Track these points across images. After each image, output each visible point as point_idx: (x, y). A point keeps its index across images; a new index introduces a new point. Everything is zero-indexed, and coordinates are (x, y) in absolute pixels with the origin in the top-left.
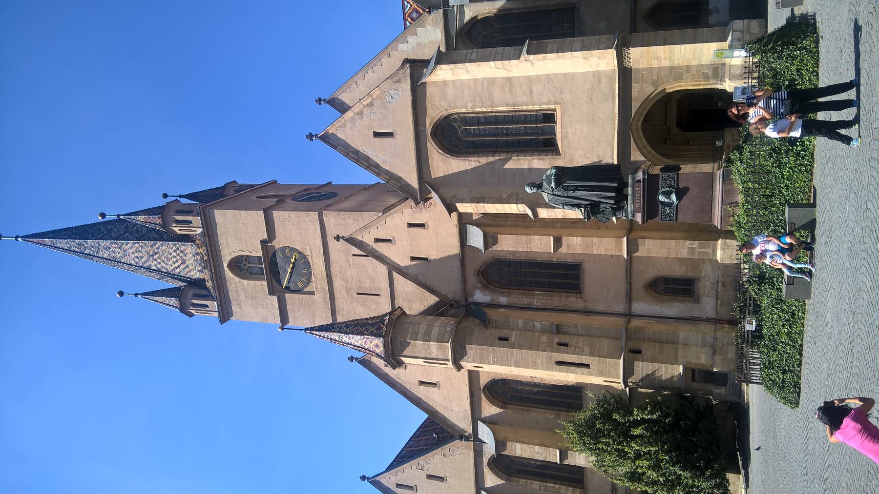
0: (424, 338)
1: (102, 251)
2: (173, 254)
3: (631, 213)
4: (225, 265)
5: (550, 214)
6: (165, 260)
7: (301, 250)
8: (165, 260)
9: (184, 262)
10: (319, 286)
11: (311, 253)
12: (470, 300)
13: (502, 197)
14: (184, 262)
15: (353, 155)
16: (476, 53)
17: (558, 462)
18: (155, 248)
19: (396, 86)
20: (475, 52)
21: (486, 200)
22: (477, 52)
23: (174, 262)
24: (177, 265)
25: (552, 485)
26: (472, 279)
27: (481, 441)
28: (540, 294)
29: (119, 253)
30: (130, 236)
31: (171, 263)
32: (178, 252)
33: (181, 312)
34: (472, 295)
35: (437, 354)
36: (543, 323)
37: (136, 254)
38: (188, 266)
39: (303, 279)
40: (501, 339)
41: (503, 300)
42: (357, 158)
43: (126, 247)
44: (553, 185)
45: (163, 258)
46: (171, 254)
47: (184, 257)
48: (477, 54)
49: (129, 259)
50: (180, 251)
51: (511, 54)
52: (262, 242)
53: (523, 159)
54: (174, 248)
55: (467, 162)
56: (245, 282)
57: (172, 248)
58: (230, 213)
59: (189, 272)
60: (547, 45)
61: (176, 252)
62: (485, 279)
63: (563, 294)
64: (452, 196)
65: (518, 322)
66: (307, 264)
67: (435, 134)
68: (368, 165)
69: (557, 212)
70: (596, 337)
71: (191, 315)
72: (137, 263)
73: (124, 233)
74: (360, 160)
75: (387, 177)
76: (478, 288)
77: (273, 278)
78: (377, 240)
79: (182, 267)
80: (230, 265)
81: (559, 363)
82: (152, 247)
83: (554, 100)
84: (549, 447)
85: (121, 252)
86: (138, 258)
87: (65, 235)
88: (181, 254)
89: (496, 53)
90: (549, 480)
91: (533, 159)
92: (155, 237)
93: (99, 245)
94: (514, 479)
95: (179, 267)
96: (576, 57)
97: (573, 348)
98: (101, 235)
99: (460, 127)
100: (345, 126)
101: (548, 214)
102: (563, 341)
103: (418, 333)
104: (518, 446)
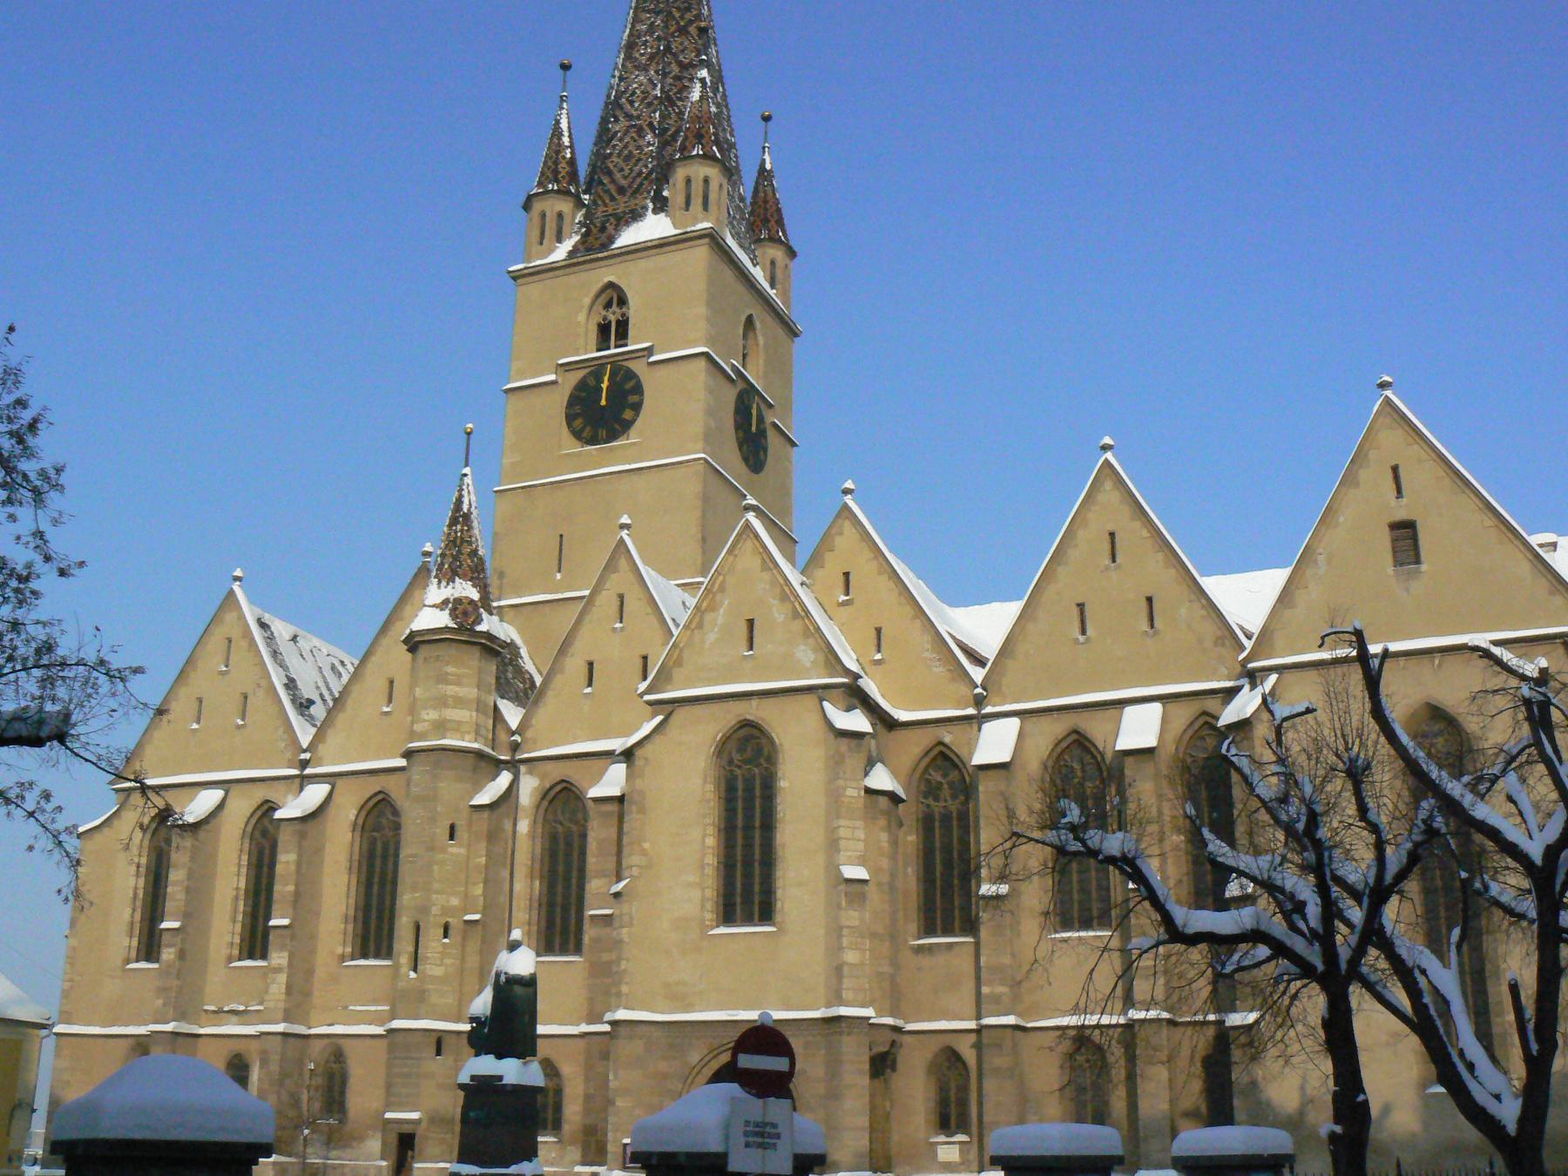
0: (451, 696)
1: (649, 18)
4: (612, 278)
7: (638, 424)
9: (621, 190)
12: (523, 768)
13: (645, 841)
14: (621, 190)
15: (718, 582)
16: (856, 795)
17: (272, 923)
19: (821, 658)
22: (859, 795)
23: (622, 170)
24: (618, 176)
25: (241, 908)
26: (557, 772)
27: (301, 789)
28: (532, 889)
29: (642, 55)
30: (673, 78)
31: (622, 164)
32: (638, 180)
34: (530, 772)
35: (425, 721)
36: (482, 898)
38: (613, 199)
39: (588, 429)
40: (452, 828)
41: (523, 826)
42: (714, 590)
46: (636, 165)
47: (628, 194)
50: (641, 184)
51: (849, 854)
52: (649, 351)
55: (701, 781)
56: (582, 317)
57: (646, 167)
58: (701, 285)
59: (606, 205)
61: (640, 173)
62: (560, 791)
63: (536, 928)
65: (481, 857)
66: (612, 436)
67: (746, 724)
68: (703, 608)
70: (461, 985)
71: (527, 206)
72: (624, 92)
73: (680, 64)
74: (711, 596)
75: (681, 645)
76: (542, 778)
77: (589, 370)
78: (621, 597)
79: (612, 188)
80: (611, 285)
81: (418, 928)
84: (295, 908)
85: (643, 60)
86: (632, 95)
90: (250, 902)
91: (703, 890)
92: (666, 130)
93: (657, 13)
94: (247, 845)
95: (613, 181)
97: (441, 949)
98: (677, 15)
100: (763, 570)
103: (458, 683)
104: (292, 857)
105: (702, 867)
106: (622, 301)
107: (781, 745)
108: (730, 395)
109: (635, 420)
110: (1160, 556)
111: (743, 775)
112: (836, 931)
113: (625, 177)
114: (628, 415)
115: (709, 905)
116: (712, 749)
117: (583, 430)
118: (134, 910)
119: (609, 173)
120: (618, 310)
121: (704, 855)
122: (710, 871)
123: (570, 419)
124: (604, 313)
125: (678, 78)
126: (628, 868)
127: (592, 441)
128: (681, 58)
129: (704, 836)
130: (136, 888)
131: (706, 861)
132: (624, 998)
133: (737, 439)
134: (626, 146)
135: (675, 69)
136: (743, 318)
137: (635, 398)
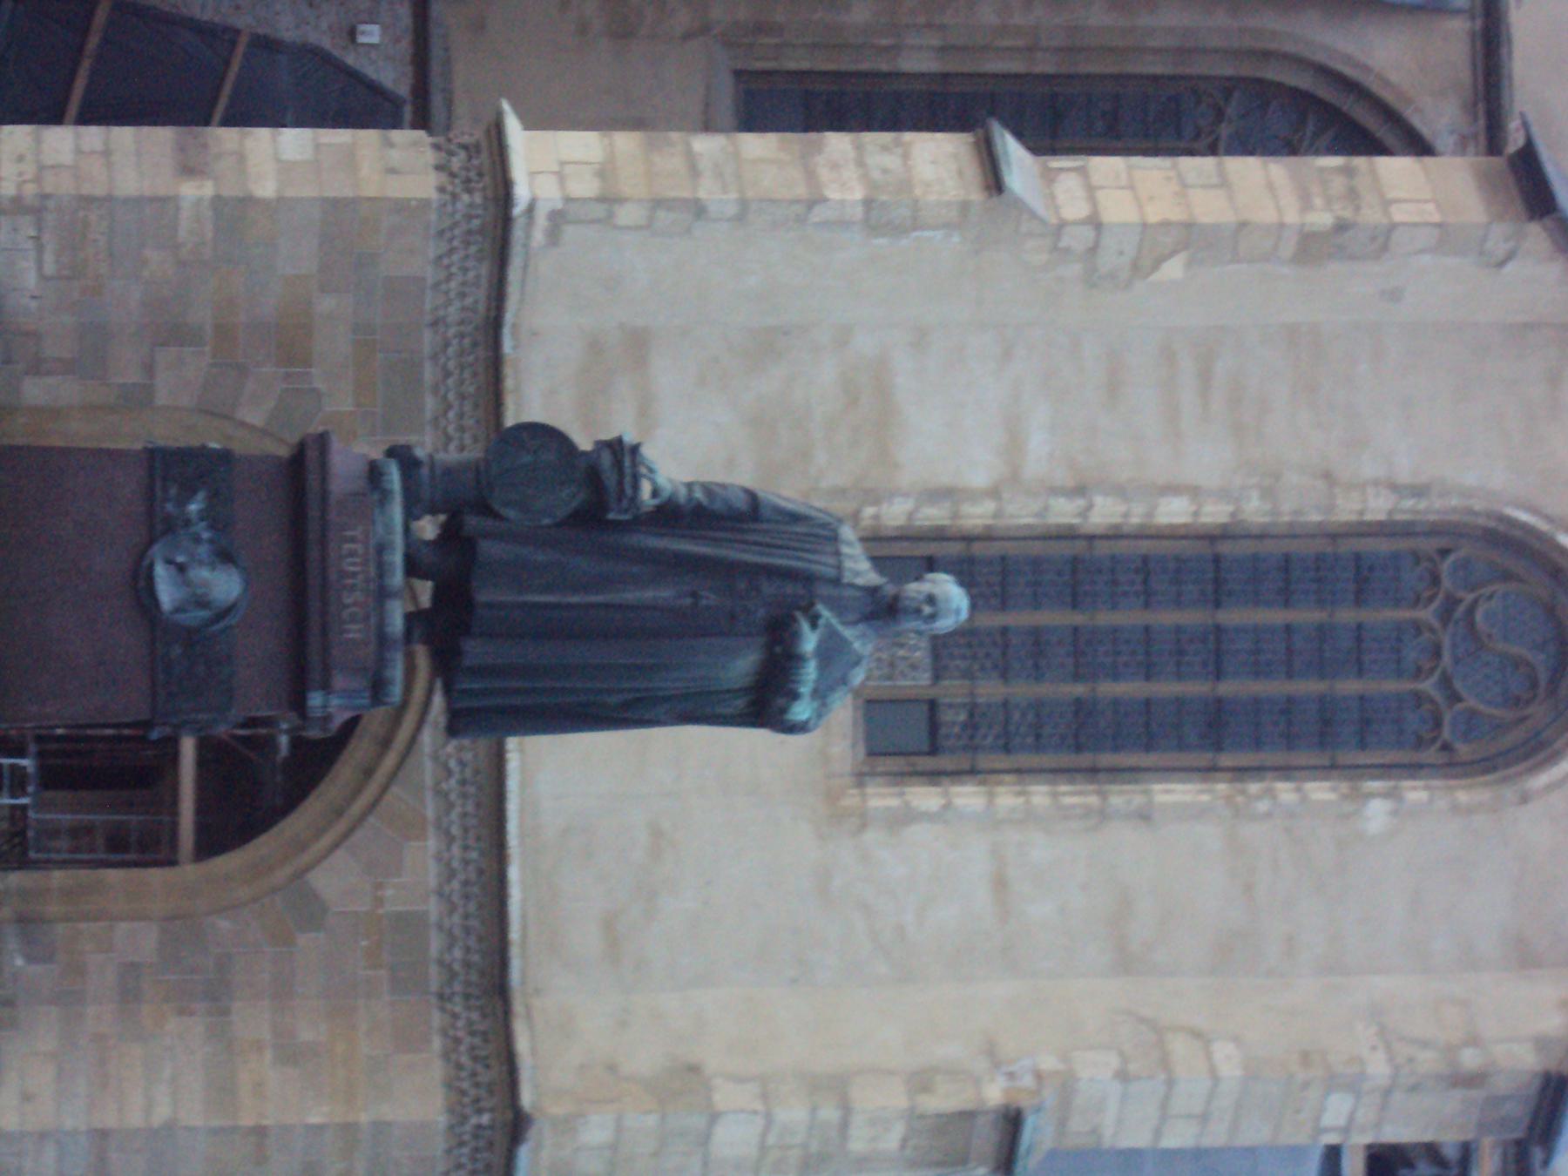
3: (385, 496)
5: (891, 161)
13: (1189, 264)
16: (1328, 1120)
20: (1327, 1130)
21: (1288, 248)
44: (809, 642)
48: (1318, 1118)
53: (1055, 491)
55: (1404, 476)
60: (908, 1152)
64: (1510, 268)
69: (850, 173)
83: (871, 836)
89: (1204, 1118)
91: (994, 493)
96: (741, 1080)
99: (1446, 682)
101: (906, 156)
105: (1080, 490)
107: (1525, 799)
111: (1418, 627)
112: (836, 1087)
115: (934, 515)
116: (1524, 517)
121: (1120, 491)
122: (1063, 512)
126: (1091, 190)
129: (1194, 492)
131: (1099, 500)
132: (599, 211)
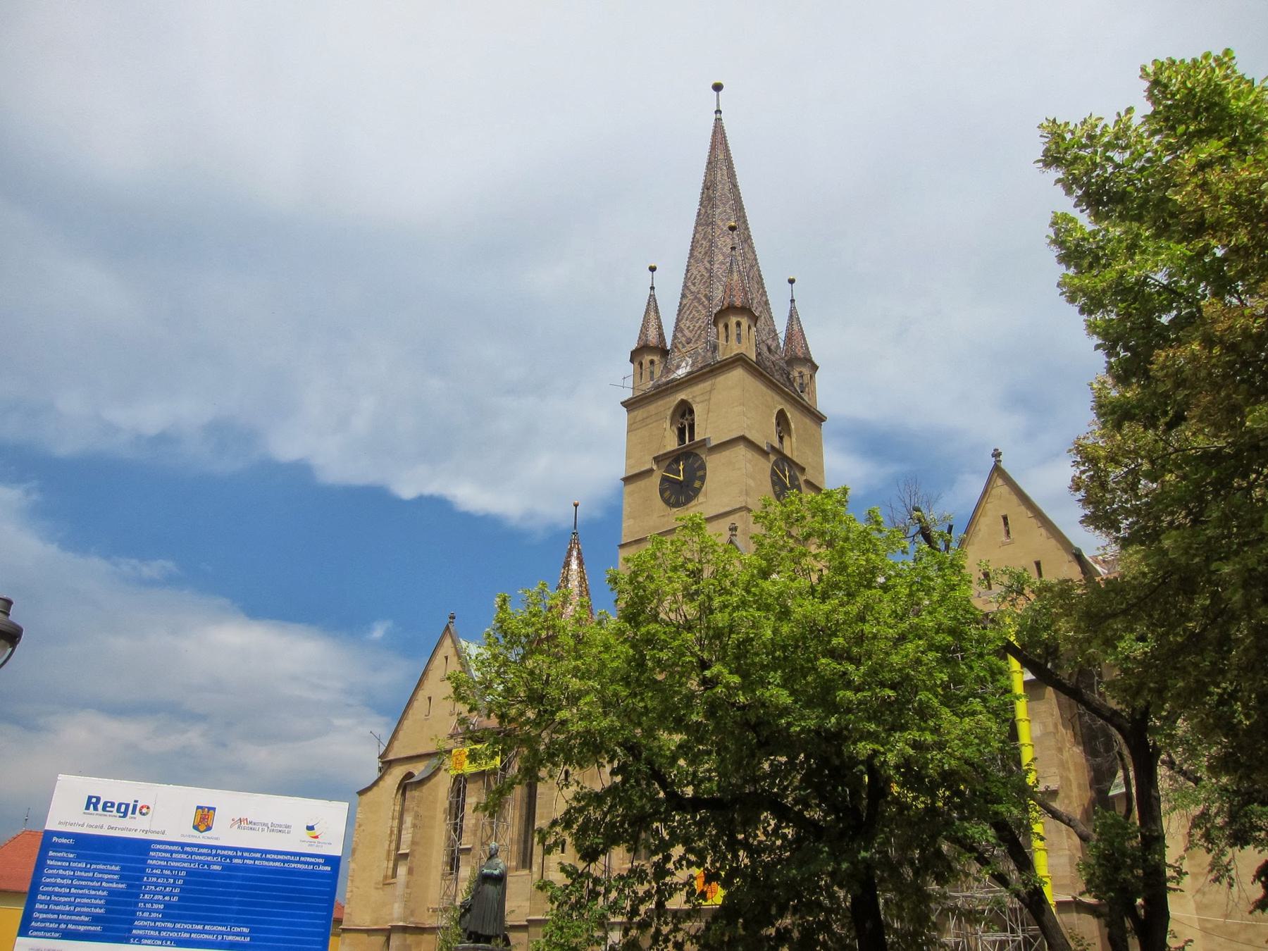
2: (698, 325)
6: (691, 316)
8: (691, 316)
10: (666, 519)
11: (702, 503)
18: (704, 299)
23: (689, 327)
24: (686, 332)
29: (700, 253)
31: (688, 323)
32: (699, 332)
33: (632, 353)
37: (698, 276)
43: (706, 262)
45: (694, 312)
49: (693, 268)
54: (703, 325)
61: (701, 326)
66: (689, 499)
71: (632, 361)
79: (684, 339)
80: (683, 402)
82: (706, 296)
86: (695, 279)
87: (722, 175)
88: (696, 336)
95: (684, 336)
98: (720, 224)
102: (566, 847)
106: (691, 412)
108: (766, 466)
109: (701, 487)
110: (1043, 531)
113: (691, 332)
114: (697, 484)
117: (670, 498)
118: (391, 842)
119: (682, 331)
120: (689, 418)
123: (662, 492)
124: (681, 420)
125: (722, 263)
127: (677, 504)
128: (724, 250)
130: (392, 827)
133: (775, 492)
134: (691, 312)
135: (721, 258)
136: (775, 412)
137: (700, 473)
